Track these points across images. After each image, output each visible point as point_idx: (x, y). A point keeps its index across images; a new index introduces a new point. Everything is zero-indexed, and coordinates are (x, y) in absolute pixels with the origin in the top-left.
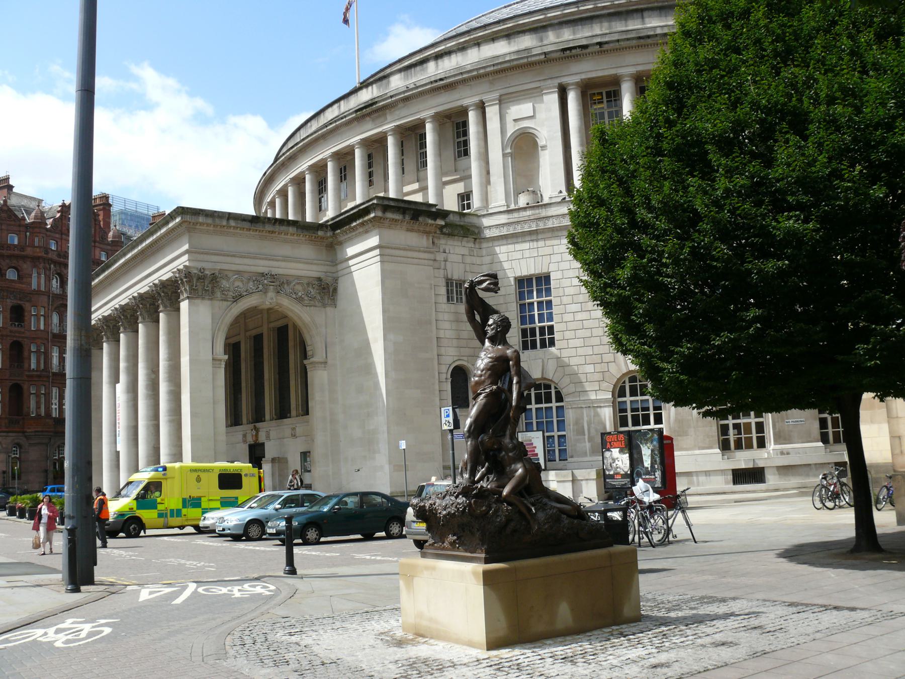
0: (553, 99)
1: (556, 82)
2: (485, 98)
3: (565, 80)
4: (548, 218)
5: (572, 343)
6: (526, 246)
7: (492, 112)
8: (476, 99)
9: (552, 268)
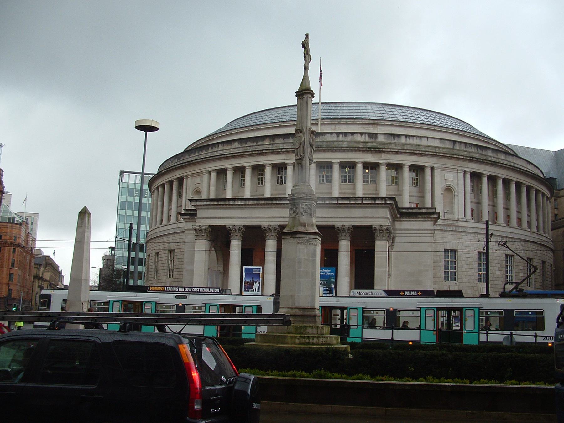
0: (461, 175)
1: (464, 169)
2: (435, 165)
3: (467, 169)
4: (459, 227)
5: (465, 281)
6: (449, 236)
7: (436, 172)
8: (432, 165)
9: (459, 248)
